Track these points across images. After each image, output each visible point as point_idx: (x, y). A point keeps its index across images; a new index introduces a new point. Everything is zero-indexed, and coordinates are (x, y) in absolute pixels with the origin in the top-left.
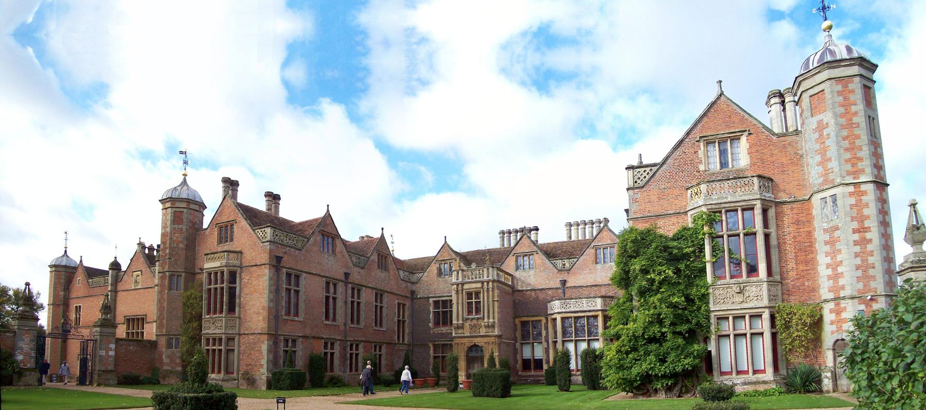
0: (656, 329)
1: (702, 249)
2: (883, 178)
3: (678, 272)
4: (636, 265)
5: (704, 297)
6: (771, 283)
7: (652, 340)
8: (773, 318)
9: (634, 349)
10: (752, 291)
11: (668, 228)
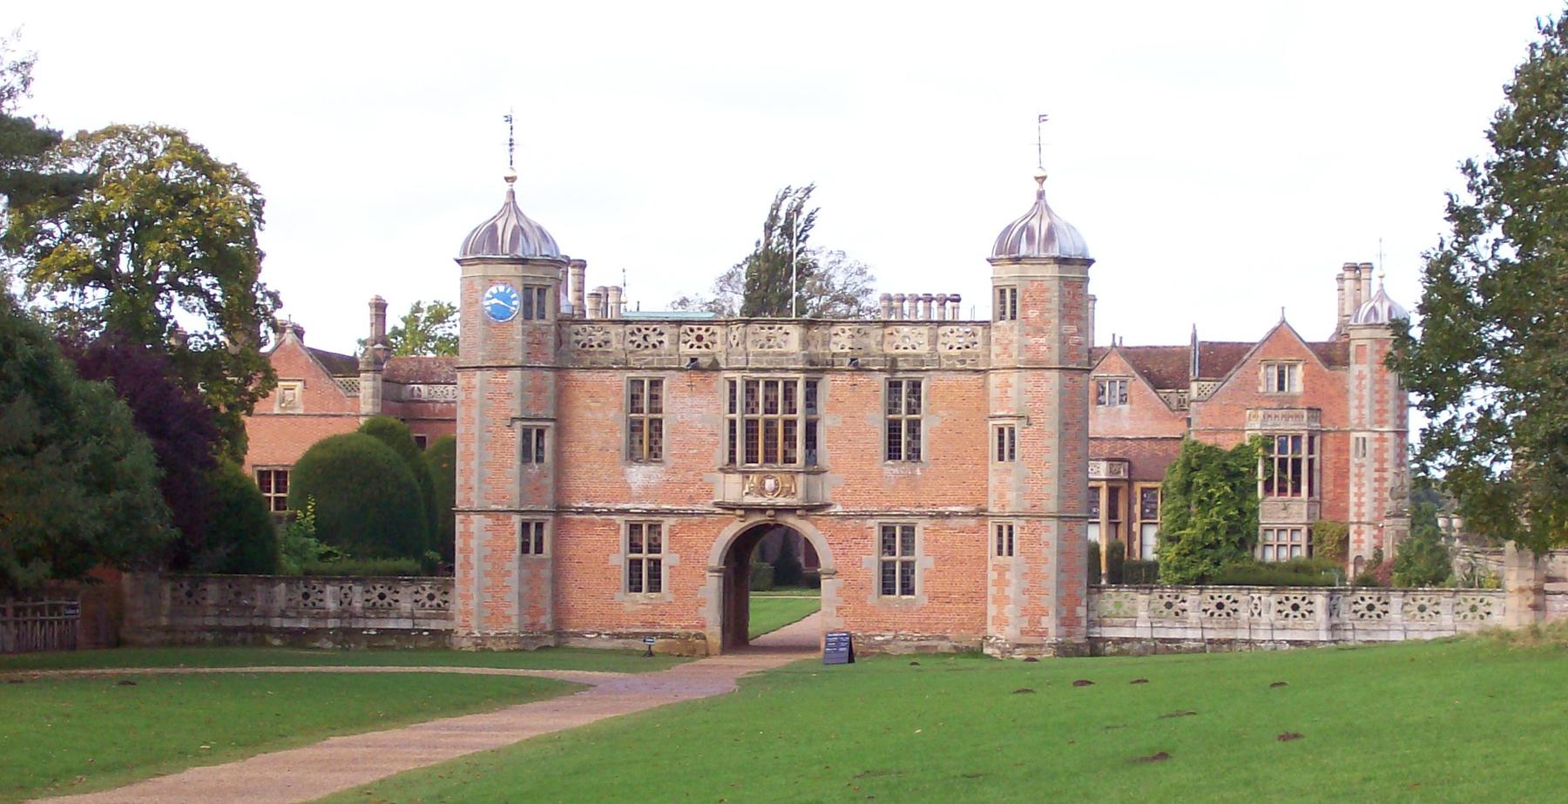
0: (1212, 538)
1: (1255, 467)
2: (1405, 426)
3: (1233, 487)
4: (1199, 479)
5: (1255, 511)
6: (1311, 503)
7: (1210, 546)
8: (1310, 532)
9: (1192, 552)
10: (1294, 508)
11: (1228, 443)
